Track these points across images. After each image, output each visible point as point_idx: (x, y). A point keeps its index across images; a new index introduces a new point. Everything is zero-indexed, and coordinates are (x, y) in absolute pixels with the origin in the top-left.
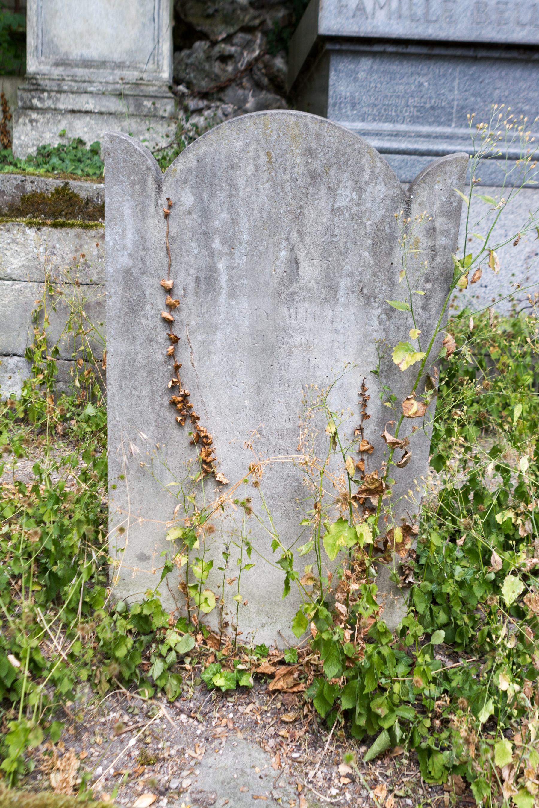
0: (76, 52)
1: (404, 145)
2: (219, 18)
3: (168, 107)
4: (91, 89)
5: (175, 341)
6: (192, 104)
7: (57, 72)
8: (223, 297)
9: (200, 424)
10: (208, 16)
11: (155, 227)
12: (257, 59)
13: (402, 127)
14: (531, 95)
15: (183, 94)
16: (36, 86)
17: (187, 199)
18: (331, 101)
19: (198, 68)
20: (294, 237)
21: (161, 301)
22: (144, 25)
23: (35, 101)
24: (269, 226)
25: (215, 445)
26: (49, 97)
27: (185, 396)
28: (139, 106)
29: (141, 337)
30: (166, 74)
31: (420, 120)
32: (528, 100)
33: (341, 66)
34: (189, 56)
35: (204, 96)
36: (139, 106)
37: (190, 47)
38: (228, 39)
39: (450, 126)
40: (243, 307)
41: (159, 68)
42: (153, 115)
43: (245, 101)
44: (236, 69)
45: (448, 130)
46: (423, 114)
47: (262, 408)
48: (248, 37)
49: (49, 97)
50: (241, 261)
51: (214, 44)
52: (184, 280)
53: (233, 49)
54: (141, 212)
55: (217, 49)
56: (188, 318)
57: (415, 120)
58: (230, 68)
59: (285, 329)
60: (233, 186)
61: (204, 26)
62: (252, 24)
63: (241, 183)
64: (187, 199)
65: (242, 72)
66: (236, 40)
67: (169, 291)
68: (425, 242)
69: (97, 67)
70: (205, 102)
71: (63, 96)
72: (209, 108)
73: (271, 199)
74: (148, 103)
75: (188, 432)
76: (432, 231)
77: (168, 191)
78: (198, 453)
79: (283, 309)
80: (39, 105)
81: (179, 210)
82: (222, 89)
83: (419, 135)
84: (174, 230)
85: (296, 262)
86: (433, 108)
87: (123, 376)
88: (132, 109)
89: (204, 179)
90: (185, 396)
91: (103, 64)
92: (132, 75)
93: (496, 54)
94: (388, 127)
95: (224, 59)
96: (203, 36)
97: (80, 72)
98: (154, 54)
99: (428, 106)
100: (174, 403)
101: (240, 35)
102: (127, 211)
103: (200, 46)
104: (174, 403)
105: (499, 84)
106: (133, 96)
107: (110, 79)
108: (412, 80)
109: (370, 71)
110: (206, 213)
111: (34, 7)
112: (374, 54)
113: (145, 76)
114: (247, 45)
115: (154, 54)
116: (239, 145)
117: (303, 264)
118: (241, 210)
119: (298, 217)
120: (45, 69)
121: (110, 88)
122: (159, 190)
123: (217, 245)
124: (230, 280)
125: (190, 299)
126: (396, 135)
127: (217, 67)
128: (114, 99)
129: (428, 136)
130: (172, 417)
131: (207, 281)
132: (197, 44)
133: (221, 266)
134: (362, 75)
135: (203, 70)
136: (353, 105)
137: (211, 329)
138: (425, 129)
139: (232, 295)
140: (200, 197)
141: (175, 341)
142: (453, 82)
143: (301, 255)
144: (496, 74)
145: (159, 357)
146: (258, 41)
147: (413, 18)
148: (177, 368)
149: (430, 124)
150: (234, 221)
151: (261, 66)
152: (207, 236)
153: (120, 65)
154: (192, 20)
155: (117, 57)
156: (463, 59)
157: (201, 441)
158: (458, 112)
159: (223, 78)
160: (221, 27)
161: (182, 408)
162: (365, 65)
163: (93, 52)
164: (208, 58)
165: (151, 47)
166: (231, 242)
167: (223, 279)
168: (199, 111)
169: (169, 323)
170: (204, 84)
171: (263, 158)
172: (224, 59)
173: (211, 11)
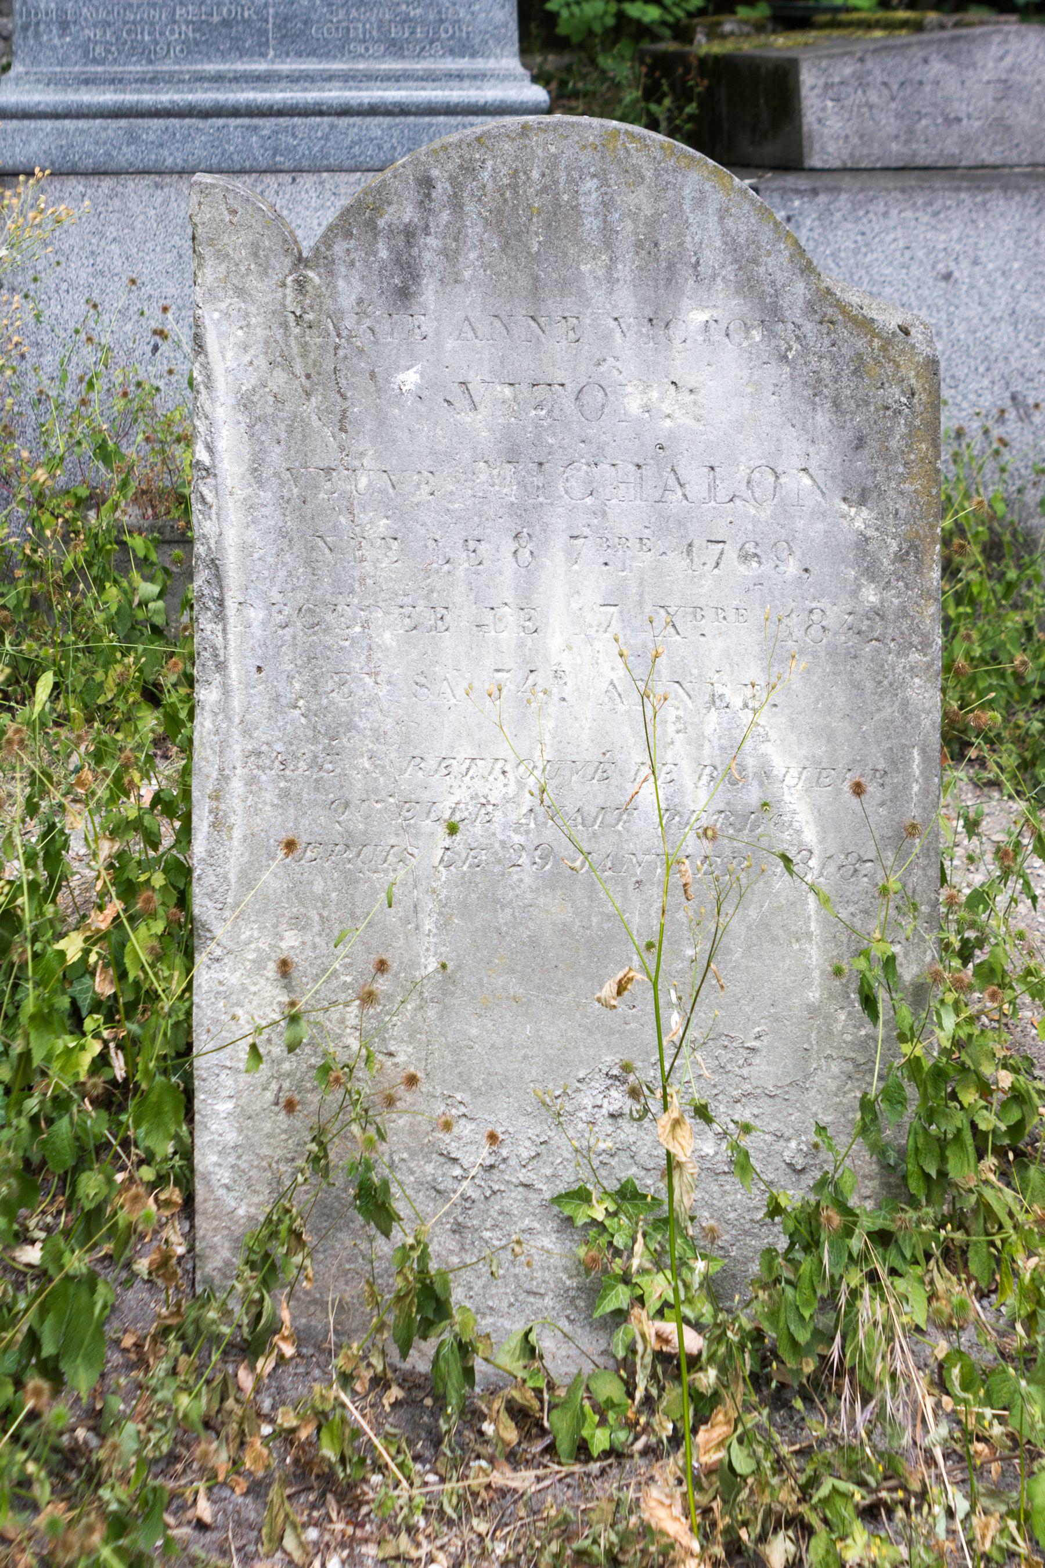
31: (203, 48)
39: (263, 55)
45: (261, 66)
57: (192, 49)
99: (216, 19)
138: (211, 68)
149: (224, 56)
158: (278, 27)
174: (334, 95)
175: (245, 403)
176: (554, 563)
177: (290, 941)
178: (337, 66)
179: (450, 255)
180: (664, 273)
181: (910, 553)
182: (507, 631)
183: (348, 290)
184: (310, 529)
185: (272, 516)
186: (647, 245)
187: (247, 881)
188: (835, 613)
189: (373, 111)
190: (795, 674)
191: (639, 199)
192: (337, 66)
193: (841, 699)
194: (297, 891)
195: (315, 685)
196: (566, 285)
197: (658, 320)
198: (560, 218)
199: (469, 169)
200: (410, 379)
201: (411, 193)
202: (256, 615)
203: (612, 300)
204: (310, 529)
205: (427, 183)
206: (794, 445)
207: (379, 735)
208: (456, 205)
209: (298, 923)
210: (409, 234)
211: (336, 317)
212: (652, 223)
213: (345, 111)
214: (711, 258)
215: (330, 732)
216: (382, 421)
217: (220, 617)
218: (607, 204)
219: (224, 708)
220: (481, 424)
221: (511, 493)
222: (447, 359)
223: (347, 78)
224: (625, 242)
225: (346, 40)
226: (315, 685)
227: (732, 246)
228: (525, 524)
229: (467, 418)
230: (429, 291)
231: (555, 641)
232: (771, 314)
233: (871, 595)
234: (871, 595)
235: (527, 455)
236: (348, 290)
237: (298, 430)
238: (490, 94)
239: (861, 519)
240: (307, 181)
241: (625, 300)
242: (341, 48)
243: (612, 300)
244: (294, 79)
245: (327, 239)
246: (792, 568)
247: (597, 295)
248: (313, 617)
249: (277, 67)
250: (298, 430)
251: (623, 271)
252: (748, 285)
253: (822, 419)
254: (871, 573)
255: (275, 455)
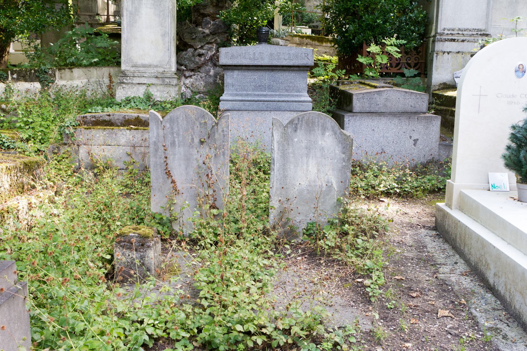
0: (140, 62)
1: (250, 99)
2: (197, 40)
3: (175, 82)
4: (145, 75)
5: (166, 158)
6: (187, 74)
7: (132, 69)
8: (177, 147)
9: (173, 178)
10: (193, 39)
11: (161, 132)
12: (213, 55)
13: (250, 93)
14: (292, 81)
15: (184, 70)
16: (124, 74)
17: (168, 125)
18: (225, 85)
19: (190, 60)
20: (192, 133)
21: (163, 148)
22: (165, 51)
23: (124, 80)
24: (187, 130)
25: (177, 183)
26: (130, 79)
27: (169, 171)
28: (164, 81)
29: (158, 157)
30: (174, 69)
32: (291, 82)
33: (228, 74)
34: (186, 54)
35: (192, 70)
36: (164, 81)
37: (186, 50)
38: (202, 47)
40: (182, 149)
41: (171, 67)
42: (169, 85)
43: (210, 71)
44: (205, 59)
45: (265, 93)
46: (258, 87)
47: (187, 173)
48: (210, 46)
49: (130, 79)
50: (181, 139)
51: (196, 49)
52: (168, 143)
53: (204, 51)
54: (158, 128)
55: (197, 52)
56: (169, 152)
58: (202, 59)
59: (192, 154)
60: (178, 122)
61: (191, 43)
62: (211, 41)
63: (180, 122)
64: (168, 125)
65: (208, 60)
66: (205, 48)
67: (164, 146)
68: (222, 134)
69: (148, 67)
70: (193, 73)
71: (135, 78)
72: (194, 75)
73: (187, 125)
74: (167, 80)
75: (170, 180)
76: (223, 131)
77: (163, 124)
78: (172, 185)
79: (191, 150)
80: (126, 82)
81: (167, 128)
82: (199, 67)
83: (255, 95)
84: (165, 132)
85: (193, 139)
86: (259, 86)
87: (154, 167)
88: (161, 83)
89: (171, 121)
90: (169, 171)
91: (150, 66)
92: (161, 70)
93: (278, 68)
94: (245, 92)
95: (200, 55)
96: (191, 46)
97: (141, 69)
98: (169, 62)
100: (166, 173)
101: (207, 45)
102: (154, 128)
103: (190, 50)
104: (166, 173)
105: (281, 77)
106: (161, 77)
107: (153, 71)
108: (252, 77)
109: (238, 75)
110: (172, 128)
111: (124, 46)
112: (238, 70)
113: (166, 70)
114: (210, 49)
115: (169, 62)
116: (179, 113)
117: (195, 139)
118: (180, 127)
119: (193, 129)
120: (128, 68)
121: (153, 75)
122: (161, 123)
123: (175, 135)
124: (178, 143)
125: (169, 148)
126: (247, 95)
127: (197, 59)
128: (154, 79)
129: (258, 95)
130: (166, 176)
131: (173, 144)
132: (189, 49)
133: (176, 140)
134: (235, 76)
135: (191, 60)
136: (233, 86)
137: (175, 155)
138: (257, 93)
139: (179, 147)
140: (170, 125)
141: (166, 158)
142: (266, 77)
143: (194, 137)
144: (280, 75)
145: (163, 162)
146: (214, 47)
147: (250, 59)
148: (167, 164)
150: (179, 130)
151: (215, 58)
152: (173, 133)
153: (156, 66)
154: (186, 40)
155: (155, 63)
156: (269, 70)
157: (173, 182)
159: (200, 63)
160: (198, 43)
161: (168, 174)
162: (236, 73)
163: (147, 61)
164: (193, 55)
165: (168, 59)
166: (178, 135)
167: (177, 143)
168: (190, 76)
169: (165, 153)
170: (192, 66)
171: (184, 116)
172: (200, 55)
173: (194, 37)
174: (277, 99)
175: (278, 142)
176: (310, 160)
177: (280, 198)
178: (277, 93)
179: (301, 127)
180: (324, 129)
181: (349, 159)
182: (305, 167)
183: (290, 130)
184: (284, 156)
185: (280, 154)
186: (322, 126)
187: (276, 193)
188: (340, 166)
189: (283, 101)
190: (335, 172)
191: (322, 121)
192: (277, 93)
193: (340, 174)
194: (281, 193)
195: (284, 172)
196: (314, 130)
197: (323, 134)
198: (313, 123)
199: (303, 117)
200: (296, 140)
201: (297, 120)
202: (278, 165)
203: (318, 132)
204: (284, 156)
205: (299, 119)
206: (337, 148)
207: (291, 177)
208: (302, 121)
209: (281, 197)
210: (297, 124)
211: (288, 133)
212: (323, 124)
213: (279, 101)
214: (329, 128)
215: (285, 177)
216: (292, 144)
217: (274, 165)
218: (318, 121)
219: (274, 174)
220: (303, 145)
221: (306, 152)
222: (300, 138)
223: (279, 95)
224: (320, 126)
225: (279, 89)
226: (284, 172)
227: (332, 126)
228: (308, 155)
229: (302, 144)
230: (298, 131)
231: (310, 168)
232: (335, 134)
233: (344, 164)
234: (344, 164)
235: (308, 148)
236: (290, 130)
237: (283, 145)
238: (302, 99)
239: (343, 156)
240: (272, 112)
241: (320, 132)
242: (279, 90)
243: (318, 132)
244: (271, 96)
245: (288, 124)
246: (336, 161)
247: (317, 131)
248: (284, 165)
249: (268, 93)
250: (283, 145)
251: (320, 129)
252: (333, 131)
253: (340, 145)
254: (344, 161)
255: (281, 148)
